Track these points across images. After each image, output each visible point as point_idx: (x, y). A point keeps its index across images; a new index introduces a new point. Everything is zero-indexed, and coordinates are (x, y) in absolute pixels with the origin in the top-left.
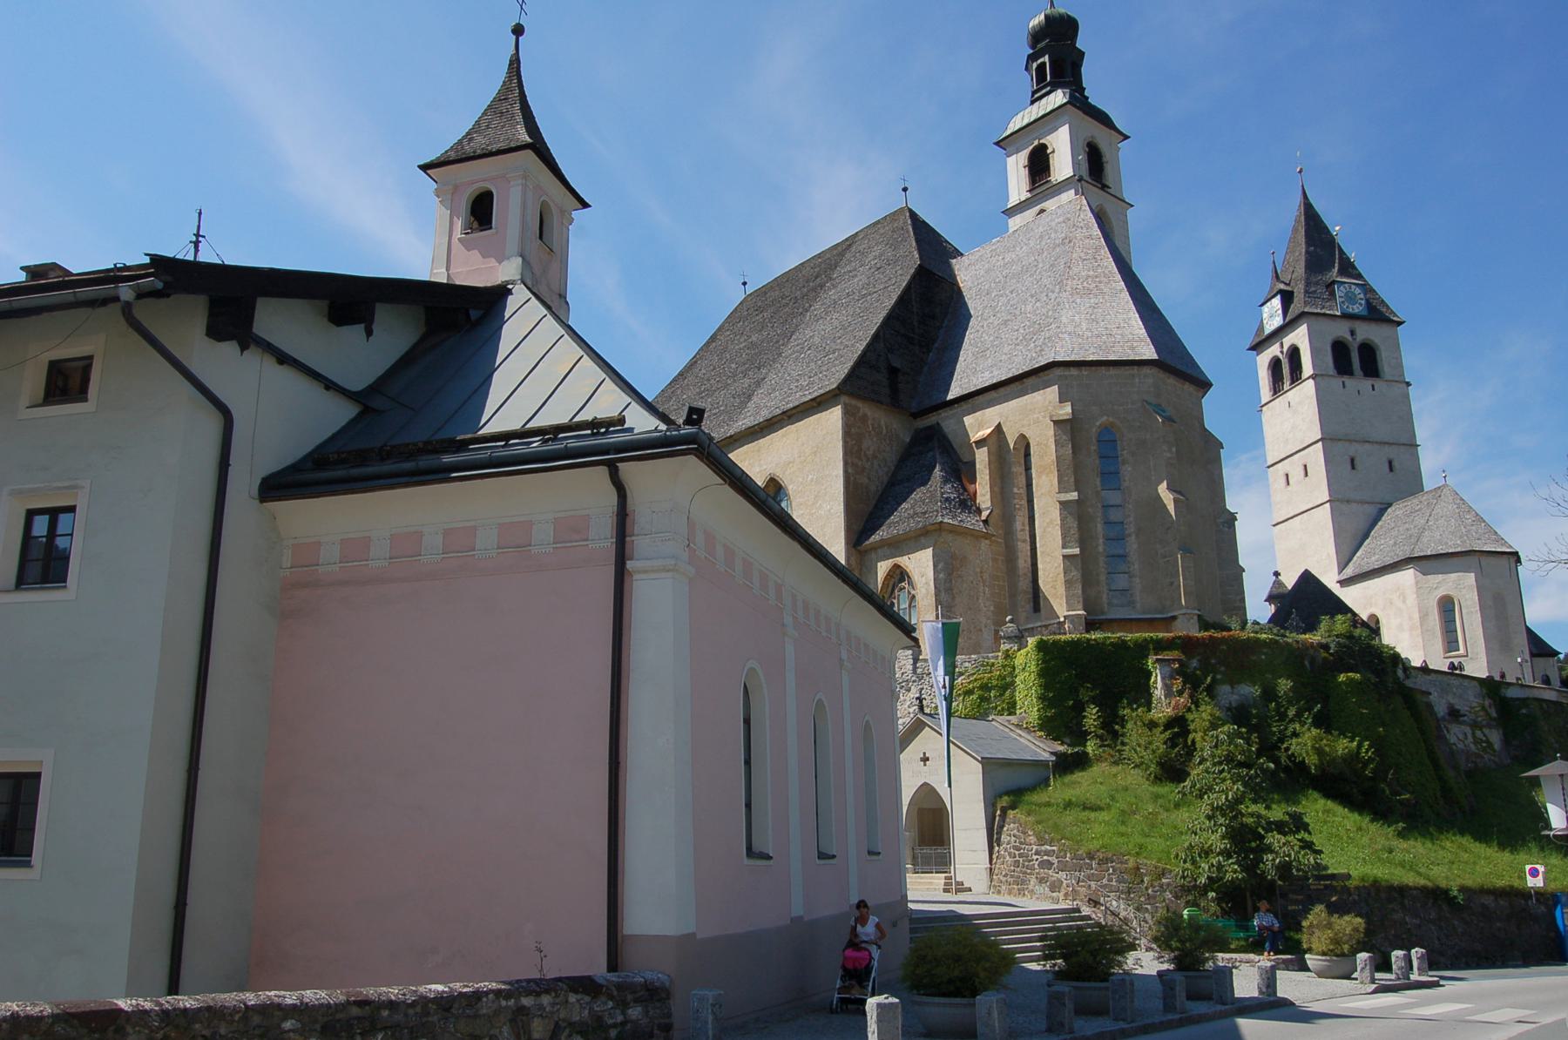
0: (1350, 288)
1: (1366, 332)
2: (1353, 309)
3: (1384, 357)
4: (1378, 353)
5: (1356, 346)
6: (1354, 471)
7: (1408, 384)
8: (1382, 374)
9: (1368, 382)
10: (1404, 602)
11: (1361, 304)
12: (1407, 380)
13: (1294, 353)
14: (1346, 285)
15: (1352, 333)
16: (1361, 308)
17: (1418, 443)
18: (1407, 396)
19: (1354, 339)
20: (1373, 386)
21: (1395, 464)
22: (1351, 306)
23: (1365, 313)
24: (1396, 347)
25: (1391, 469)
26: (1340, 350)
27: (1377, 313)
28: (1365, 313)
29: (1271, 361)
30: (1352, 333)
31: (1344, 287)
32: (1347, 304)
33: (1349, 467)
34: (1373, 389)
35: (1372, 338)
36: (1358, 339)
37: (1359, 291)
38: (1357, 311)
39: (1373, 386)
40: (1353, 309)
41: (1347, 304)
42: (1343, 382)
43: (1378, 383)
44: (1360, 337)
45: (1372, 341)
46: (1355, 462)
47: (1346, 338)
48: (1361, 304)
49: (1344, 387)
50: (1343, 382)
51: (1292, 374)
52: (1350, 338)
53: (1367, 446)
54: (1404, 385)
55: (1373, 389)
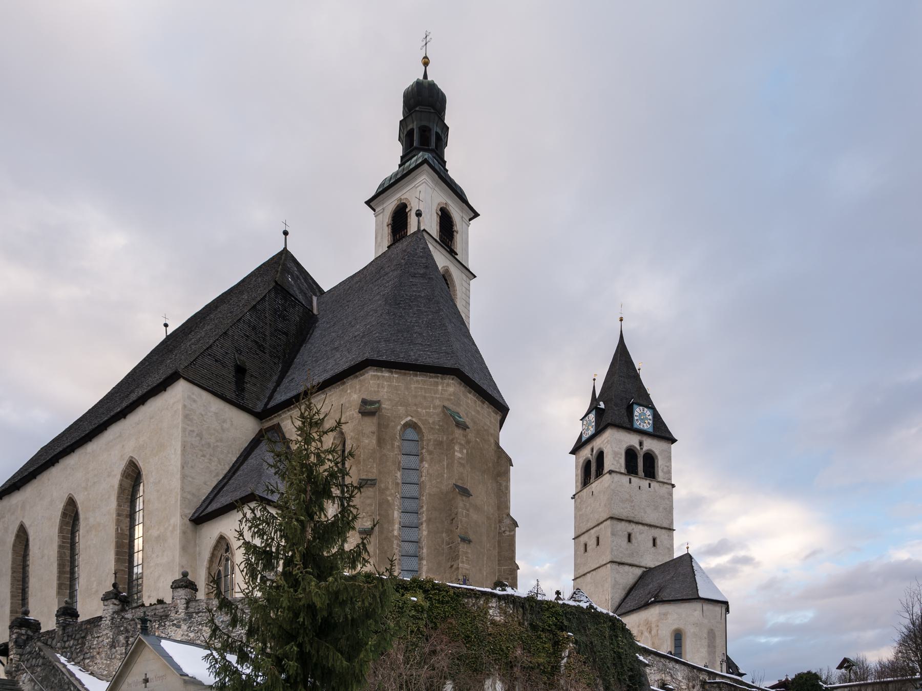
0: (643, 411)
1: (650, 445)
2: (643, 426)
3: (660, 463)
4: (656, 461)
5: (642, 454)
6: (630, 544)
7: (673, 486)
8: (657, 476)
9: (645, 483)
10: (650, 632)
11: (649, 423)
12: (673, 483)
13: (600, 456)
14: (641, 408)
15: (641, 444)
16: (649, 426)
17: (674, 529)
18: (671, 494)
19: (642, 449)
20: (650, 484)
21: (658, 542)
22: (642, 424)
23: (651, 430)
24: (669, 459)
25: (654, 545)
26: (630, 454)
27: (662, 432)
28: (651, 430)
29: (584, 461)
30: (641, 444)
31: (640, 409)
32: (639, 422)
33: (626, 540)
34: (650, 487)
35: (654, 449)
36: (644, 449)
37: (649, 414)
38: (646, 428)
39: (650, 484)
40: (643, 426)
41: (639, 422)
42: (630, 479)
43: (653, 484)
44: (645, 448)
45: (654, 452)
46: (631, 537)
47: (635, 447)
48: (649, 423)
49: (630, 483)
50: (630, 479)
51: (597, 471)
52: (638, 448)
53: (640, 527)
54: (670, 487)
55: (650, 487)
